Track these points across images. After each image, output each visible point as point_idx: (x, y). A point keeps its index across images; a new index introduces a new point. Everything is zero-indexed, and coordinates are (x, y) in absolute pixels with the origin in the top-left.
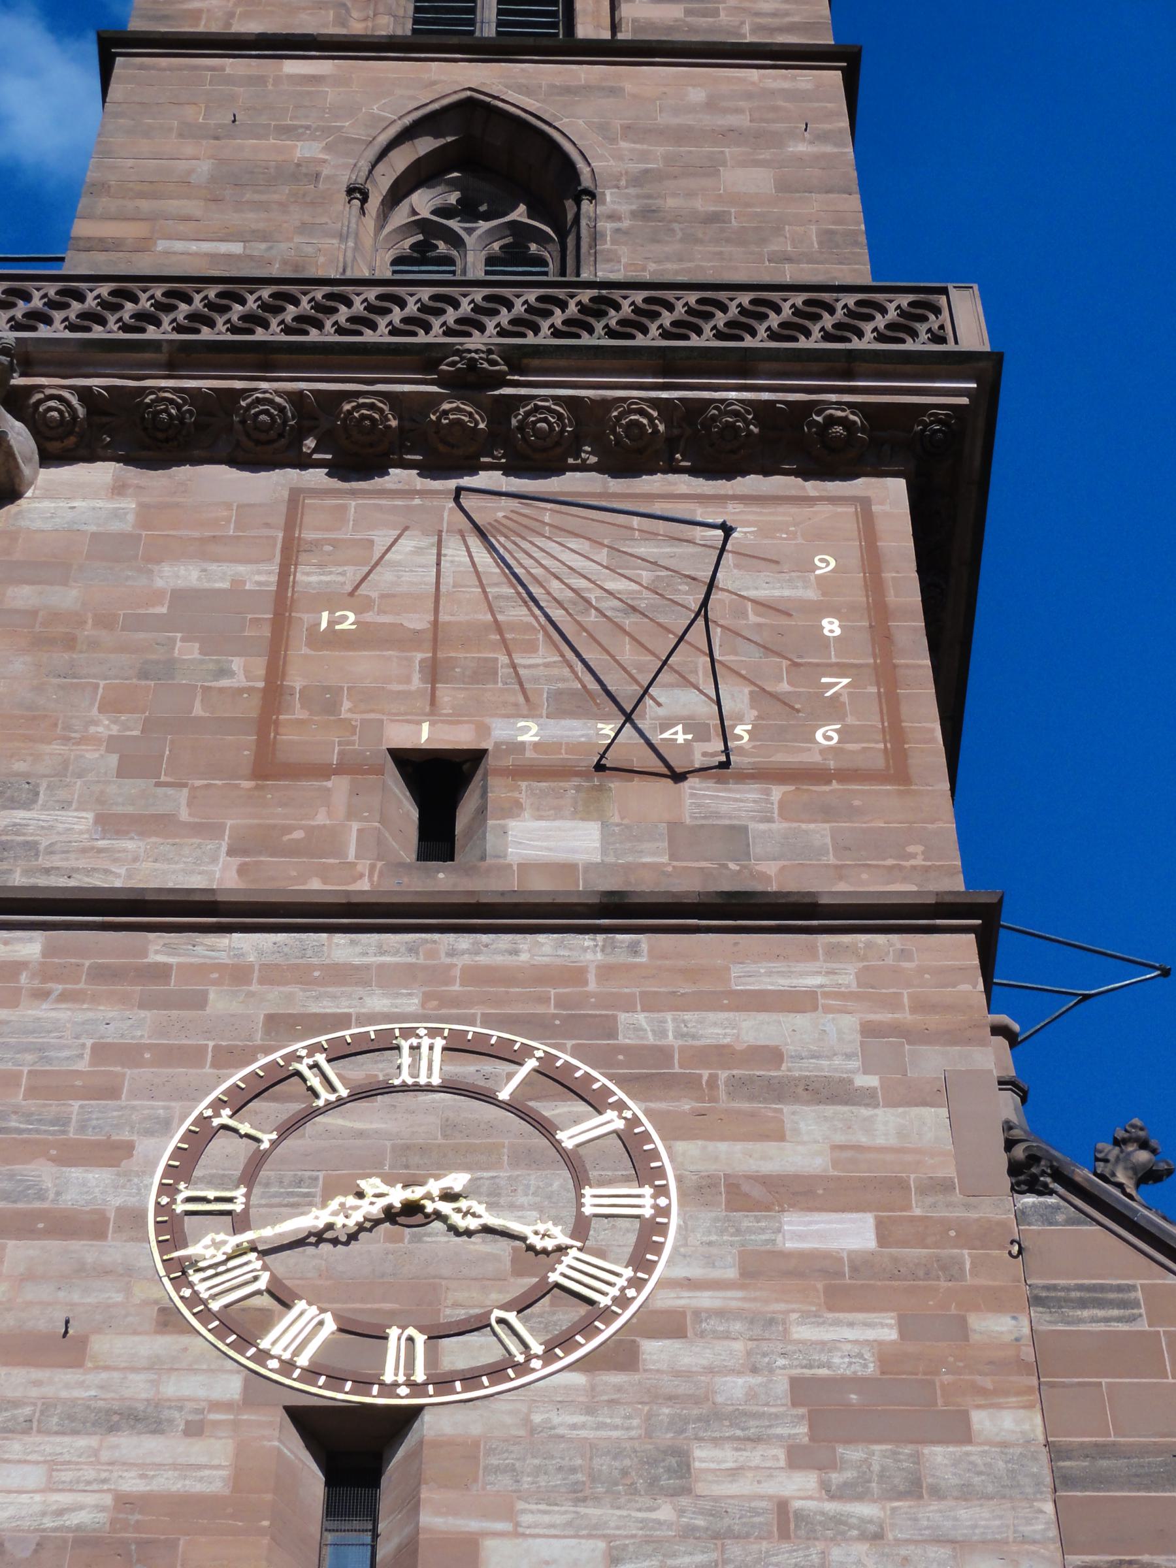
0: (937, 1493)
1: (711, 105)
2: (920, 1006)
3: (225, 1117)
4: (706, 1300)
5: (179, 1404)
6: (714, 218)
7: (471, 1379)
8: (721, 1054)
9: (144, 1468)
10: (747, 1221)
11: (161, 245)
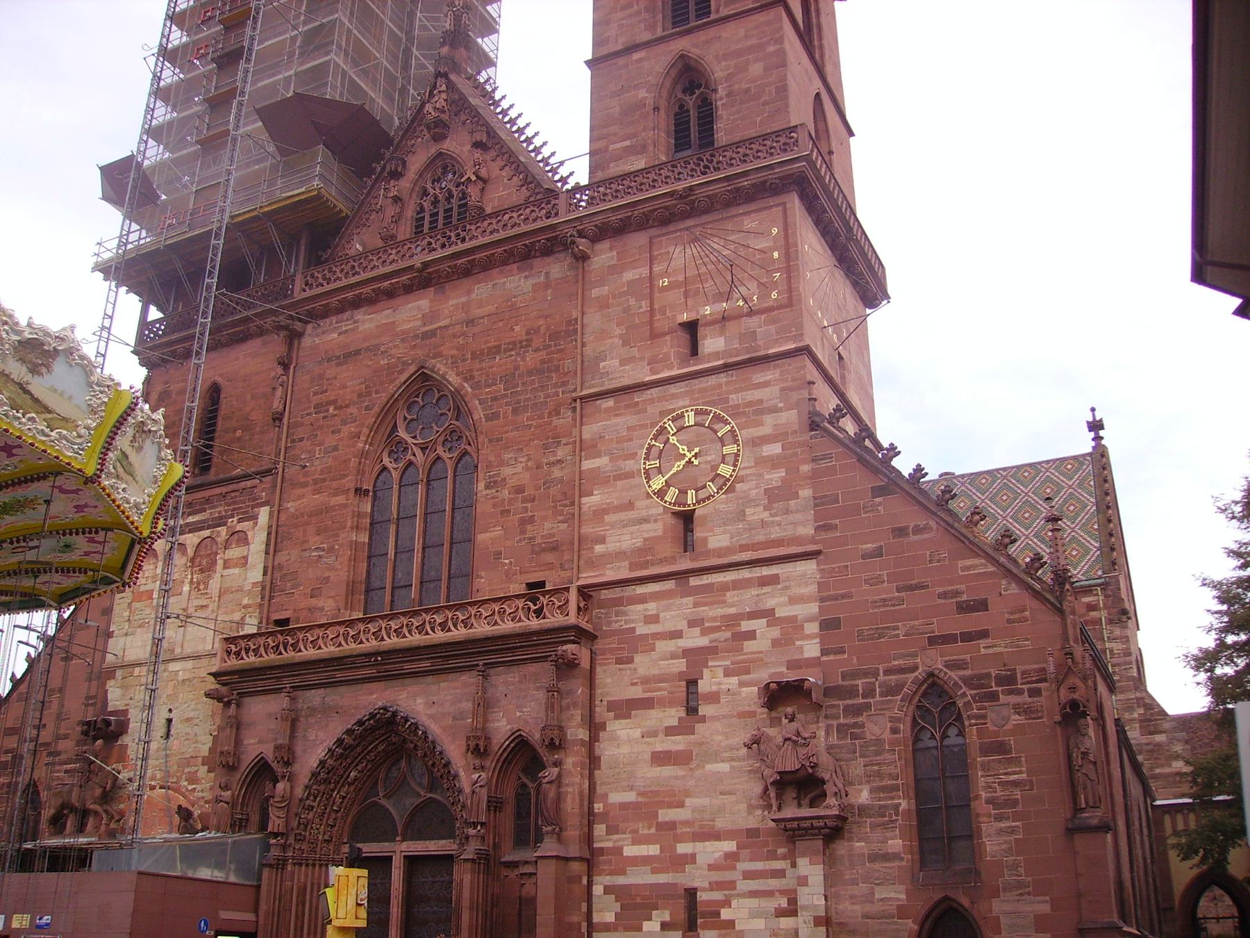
0: (792, 512)
1: (746, 37)
3: (653, 443)
4: (748, 472)
5: (652, 515)
6: (748, 90)
7: (704, 500)
8: (750, 404)
9: (647, 532)
11: (611, 147)
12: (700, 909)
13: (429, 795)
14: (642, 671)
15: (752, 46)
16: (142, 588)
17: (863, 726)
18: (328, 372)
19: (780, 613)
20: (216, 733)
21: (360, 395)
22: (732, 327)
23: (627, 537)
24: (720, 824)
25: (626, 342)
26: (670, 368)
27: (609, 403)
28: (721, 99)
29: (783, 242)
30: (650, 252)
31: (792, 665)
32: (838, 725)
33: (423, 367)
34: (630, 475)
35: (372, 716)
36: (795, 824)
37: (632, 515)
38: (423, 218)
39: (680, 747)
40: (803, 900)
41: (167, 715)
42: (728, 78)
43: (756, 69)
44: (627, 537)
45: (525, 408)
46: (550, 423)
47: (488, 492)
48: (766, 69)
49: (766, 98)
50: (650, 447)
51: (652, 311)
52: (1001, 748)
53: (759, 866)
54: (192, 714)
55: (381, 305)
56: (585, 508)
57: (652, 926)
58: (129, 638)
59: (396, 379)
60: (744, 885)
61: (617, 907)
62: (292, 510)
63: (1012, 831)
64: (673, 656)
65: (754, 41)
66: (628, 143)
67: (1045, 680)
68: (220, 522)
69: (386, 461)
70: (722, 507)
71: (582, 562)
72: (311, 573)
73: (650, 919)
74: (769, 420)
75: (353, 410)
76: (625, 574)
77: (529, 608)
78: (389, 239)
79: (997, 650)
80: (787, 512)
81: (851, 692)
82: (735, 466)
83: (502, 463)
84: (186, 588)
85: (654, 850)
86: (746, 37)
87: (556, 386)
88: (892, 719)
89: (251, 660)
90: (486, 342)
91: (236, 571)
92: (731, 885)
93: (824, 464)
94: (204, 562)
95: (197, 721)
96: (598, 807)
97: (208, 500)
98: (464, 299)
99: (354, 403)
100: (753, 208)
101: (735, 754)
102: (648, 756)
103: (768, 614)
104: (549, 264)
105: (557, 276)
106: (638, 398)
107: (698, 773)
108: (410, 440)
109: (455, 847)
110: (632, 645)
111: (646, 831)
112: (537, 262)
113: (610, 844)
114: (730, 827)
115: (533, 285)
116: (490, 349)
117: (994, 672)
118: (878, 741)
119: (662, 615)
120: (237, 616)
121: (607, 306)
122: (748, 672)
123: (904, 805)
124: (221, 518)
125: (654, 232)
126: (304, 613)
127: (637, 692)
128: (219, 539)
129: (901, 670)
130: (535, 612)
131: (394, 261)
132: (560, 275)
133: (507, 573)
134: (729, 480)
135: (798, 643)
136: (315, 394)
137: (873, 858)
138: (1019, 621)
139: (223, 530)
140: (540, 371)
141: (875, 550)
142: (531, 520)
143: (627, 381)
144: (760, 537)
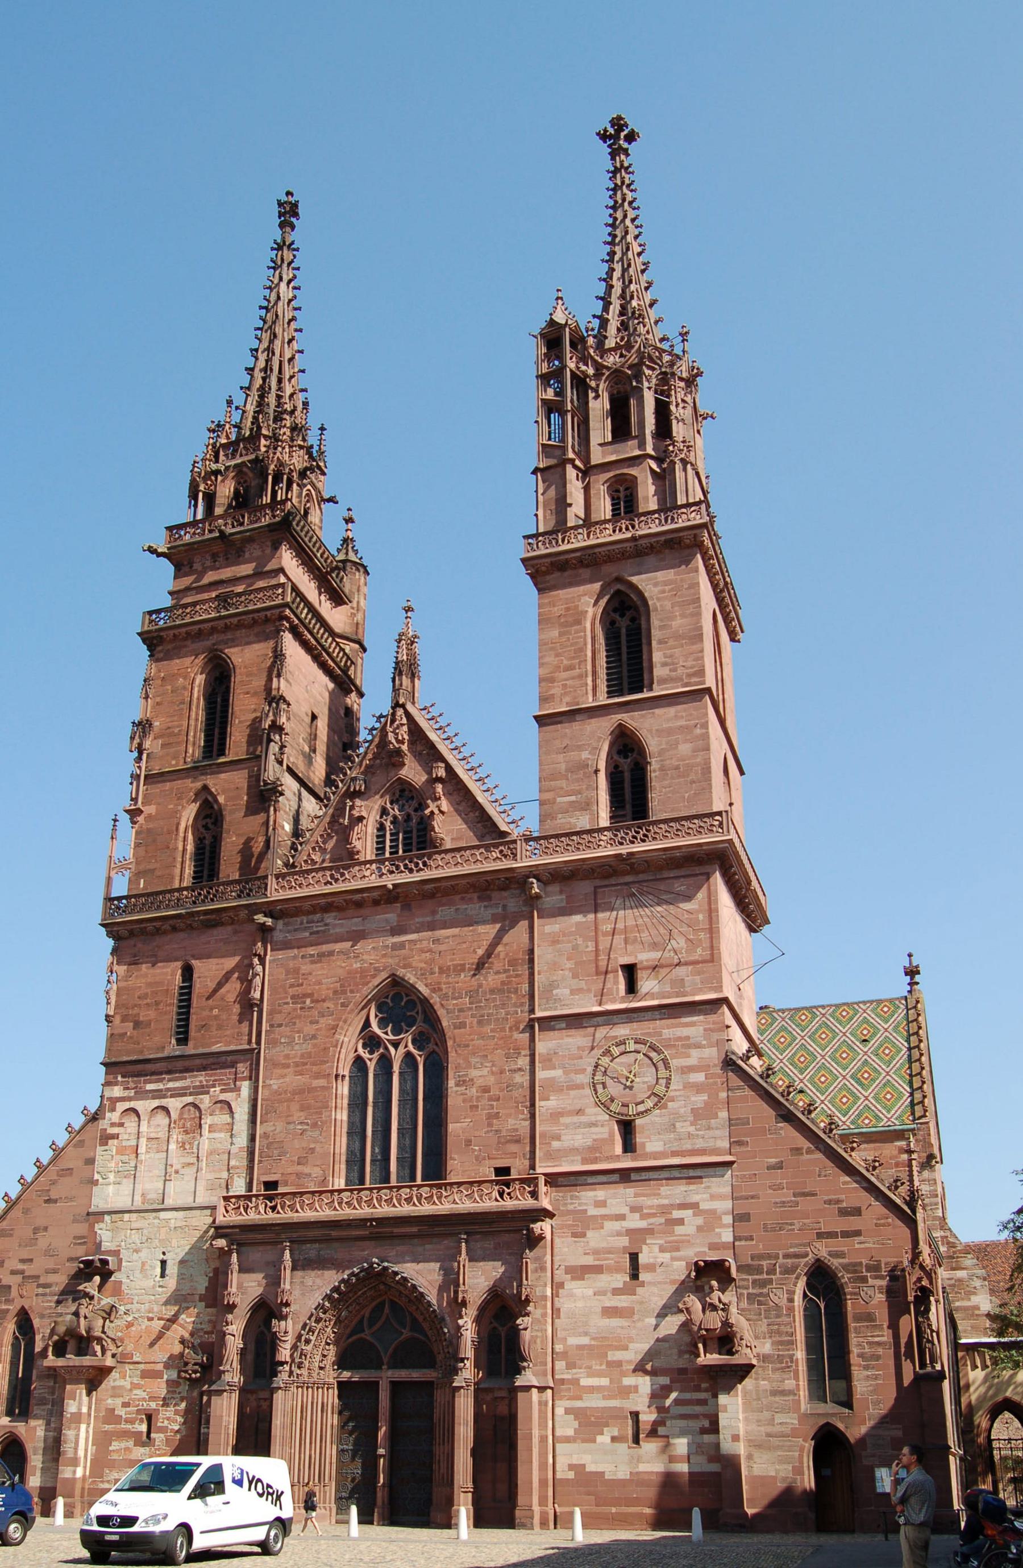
2: (714, 1023)
4: (678, 1093)
6: (677, 768)
7: (642, 1113)
8: (680, 1039)
9: (596, 1134)
10: (684, 1076)
11: (559, 800)
14: (593, 1244)
16: (124, 1143)
18: (303, 967)
19: (703, 1206)
20: (211, 1275)
21: (335, 992)
22: (663, 972)
25: (575, 976)
28: (655, 771)
29: (706, 907)
31: (713, 1247)
32: (748, 1294)
33: (394, 975)
37: (583, 1119)
39: (625, 1304)
42: (661, 753)
44: (580, 1137)
45: (489, 1022)
46: (511, 1037)
47: (458, 1088)
49: (692, 777)
53: (688, 1396)
55: (350, 912)
57: (604, 1439)
59: (369, 982)
61: (576, 1424)
62: (275, 1087)
64: (619, 1234)
66: (573, 798)
68: (203, 1090)
70: (657, 1119)
72: (297, 1144)
74: (695, 1053)
75: (329, 1004)
77: (504, 1191)
80: (709, 1128)
83: (469, 1065)
85: (604, 1382)
87: (515, 1005)
89: (252, 1217)
90: (452, 960)
91: (222, 1135)
94: (188, 1125)
97: (187, 1070)
98: (429, 919)
99: (330, 999)
100: (683, 874)
103: (694, 1206)
104: (506, 898)
105: (513, 910)
107: (639, 1324)
111: (598, 1367)
112: (495, 894)
113: (569, 1377)
115: (493, 915)
116: (455, 966)
119: (608, 1201)
121: (558, 942)
122: (678, 1249)
124: (202, 1087)
125: (598, 882)
126: (293, 1177)
127: (589, 1260)
128: (202, 1106)
129: (796, 1256)
130: (509, 1194)
131: (364, 876)
132: (516, 909)
133: (477, 1158)
135: (717, 1230)
136: (292, 986)
139: (206, 1098)
140: (501, 991)
142: (497, 1116)
144: (688, 1146)
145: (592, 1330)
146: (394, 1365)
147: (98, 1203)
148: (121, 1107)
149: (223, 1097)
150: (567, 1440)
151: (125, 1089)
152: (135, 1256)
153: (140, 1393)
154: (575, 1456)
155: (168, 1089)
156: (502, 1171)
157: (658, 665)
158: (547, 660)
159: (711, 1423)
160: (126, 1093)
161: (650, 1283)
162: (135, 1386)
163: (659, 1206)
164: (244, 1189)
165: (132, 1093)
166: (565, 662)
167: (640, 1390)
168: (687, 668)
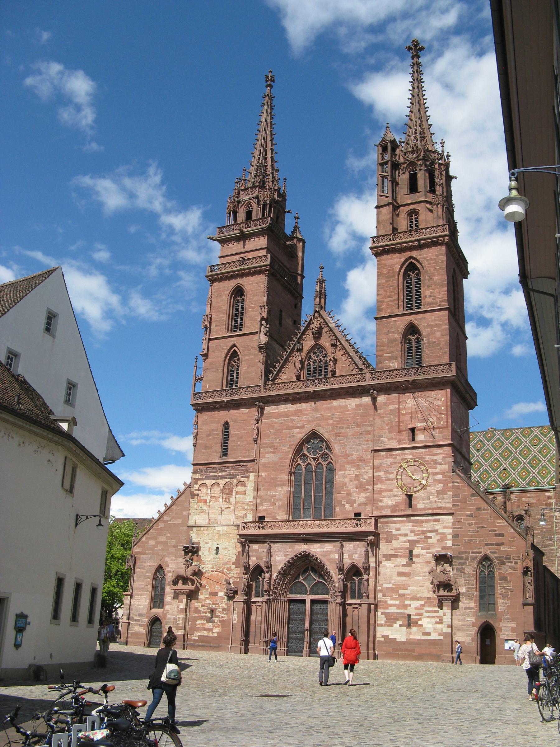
1: (435, 320)
4: (431, 484)
6: (435, 342)
7: (416, 491)
8: (432, 460)
10: (434, 476)
12: (412, 621)
13: (319, 580)
15: (437, 324)
16: (202, 498)
17: (464, 569)
23: (390, 501)
24: (419, 595)
26: (405, 444)
27: (384, 453)
28: (425, 344)
29: (445, 404)
30: (399, 400)
31: (443, 548)
34: (391, 480)
35: (301, 554)
36: (443, 598)
37: (392, 493)
38: (310, 368)
40: (444, 620)
41: (217, 546)
42: (428, 335)
43: (438, 334)
44: (390, 501)
48: (442, 335)
49: (441, 347)
50: (398, 471)
51: (399, 422)
52: (505, 579)
54: (227, 547)
56: (375, 489)
57: (396, 625)
58: (197, 516)
60: (426, 614)
61: (385, 619)
62: (264, 476)
63: (507, 603)
65: (437, 322)
66: (390, 355)
67: (519, 560)
68: (233, 477)
69: (300, 462)
71: (374, 508)
73: (396, 623)
76: (388, 513)
78: (298, 377)
79: (506, 549)
80: (443, 499)
81: (461, 558)
82: (427, 481)
84: (221, 500)
85: (397, 602)
86: (435, 320)
88: (473, 567)
91: (242, 496)
92: (422, 614)
93: (456, 484)
94: (228, 491)
95: (229, 549)
96: (379, 588)
101: (424, 574)
102: (396, 573)
103: (436, 531)
106: (394, 453)
107: (412, 579)
108: (309, 456)
109: (329, 597)
110: (391, 537)
114: (422, 596)
117: (504, 556)
118: (469, 574)
119: (401, 528)
120: (243, 513)
121: (383, 417)
122: (429, 549)
123: (475, 593)
124: (233, 475)
127: (393, 553)
130: (360, 525)
134: (424, 486)
137: (466, 608)
138: (513, 541)
139: (235, 481)
141: (471, 514)
143: (390, 447)
144: (434, 506)
145: (393, 581)
146: (312, 592)
147: (191, 522)
148: (200, 482)
149: (242, 479)
150: (382, 625)
151: (201, 475)
152: (206, 545)
153: (208, 601)
154: (385, 632)
155: (219, 476)
156: (358, 515)
157: (428, 297)
158: (380, 292)
159: (440, 620)
160: (202, 477)
161: (417, 562)
162: (206, 598)
163: (422, 531)
164: (251, 519)
165: (204, 477)
166: (388, 294)
167: (412, 606)
168: (440, 298)
